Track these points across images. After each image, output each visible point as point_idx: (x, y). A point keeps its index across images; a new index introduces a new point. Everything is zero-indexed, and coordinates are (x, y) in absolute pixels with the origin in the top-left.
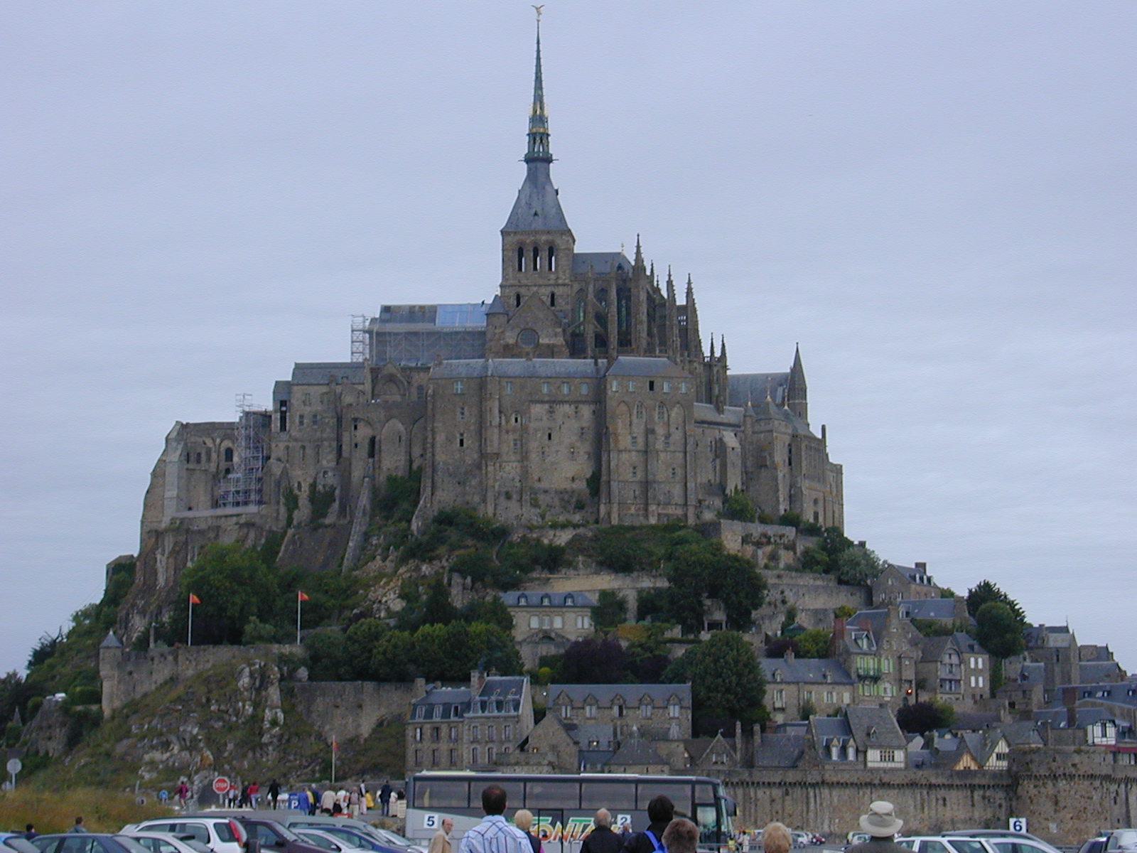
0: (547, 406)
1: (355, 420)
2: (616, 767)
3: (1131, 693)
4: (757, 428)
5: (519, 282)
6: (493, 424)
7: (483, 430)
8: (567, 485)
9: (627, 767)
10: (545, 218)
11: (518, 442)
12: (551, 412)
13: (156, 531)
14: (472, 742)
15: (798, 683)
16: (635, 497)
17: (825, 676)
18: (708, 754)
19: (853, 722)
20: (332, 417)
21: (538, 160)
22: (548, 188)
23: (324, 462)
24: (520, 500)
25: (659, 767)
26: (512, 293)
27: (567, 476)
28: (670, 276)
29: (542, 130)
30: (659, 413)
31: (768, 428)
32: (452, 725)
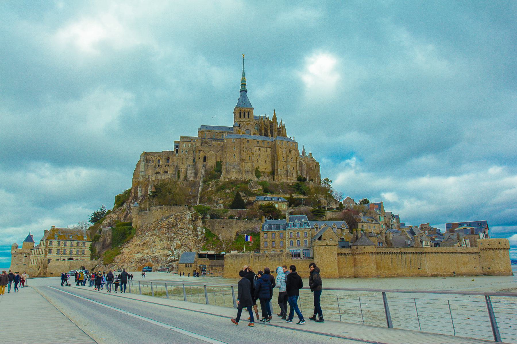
0: (258, 148)
1: (199, 151)
2: (360, 246)
3: (479, 224)
4: (308, 160)
6: (245, 151)
9: (365, 246)
11: (251, 157)
12: (259, 149)
13: (138, 181)
15: (367, 223)
21: (244, 91)
22: (247, 98)
24: (252, 174)
26: (239, 123)
28: (281, 121)
31: (312, 159)
32: (280, 232)
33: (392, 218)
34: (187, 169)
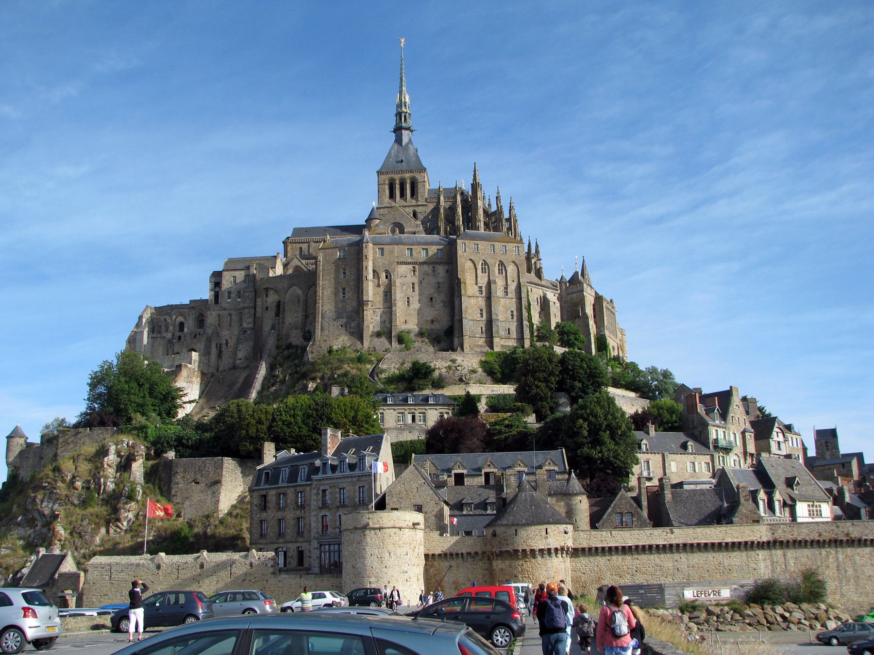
0: (411, 267)
1: (267, 289)
2: (503, 529)
5: (391, 205)
7: (360, 283)
8: (429, 326)
10: (408, 163)
14: (320, 508)
16: (482, 332)
17: (684, 446)
18: (610, 515)
19: (771, 472)
20: (251, 292)
22: (410, 146)
23: (245, 325)
25: (562, 527)
27: (428, 319)
29: (405, 111)
30: (499, 269)
32: (299, 489)
33: (781, 435)
34: (239, 341)
